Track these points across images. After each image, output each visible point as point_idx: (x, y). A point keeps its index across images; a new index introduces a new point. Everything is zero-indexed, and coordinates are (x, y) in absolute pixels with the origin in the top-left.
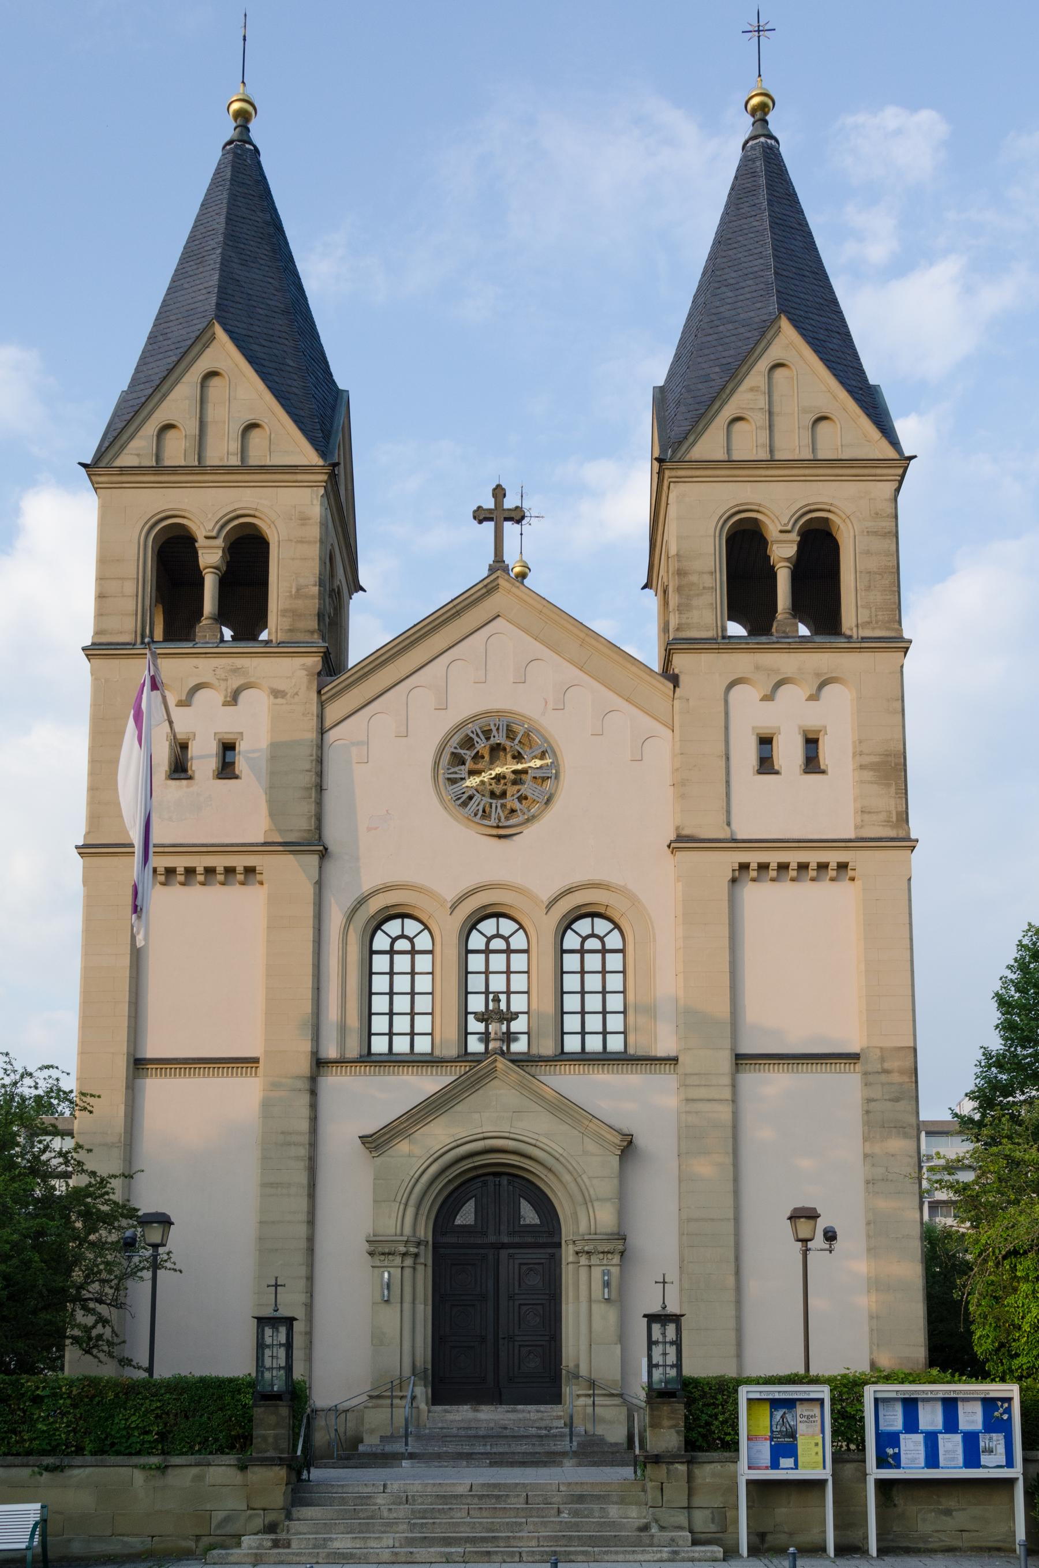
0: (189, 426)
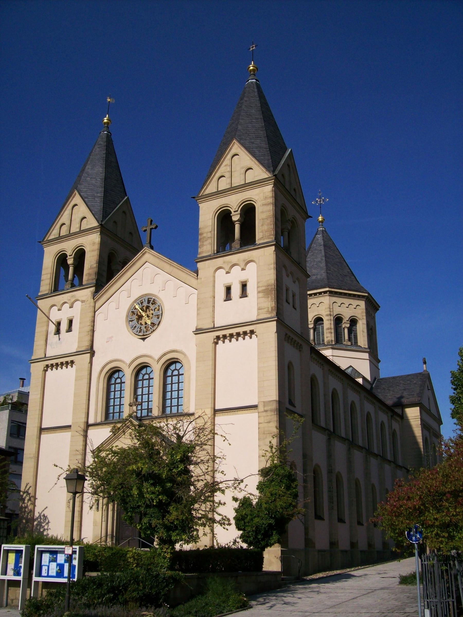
0: (68, 223)
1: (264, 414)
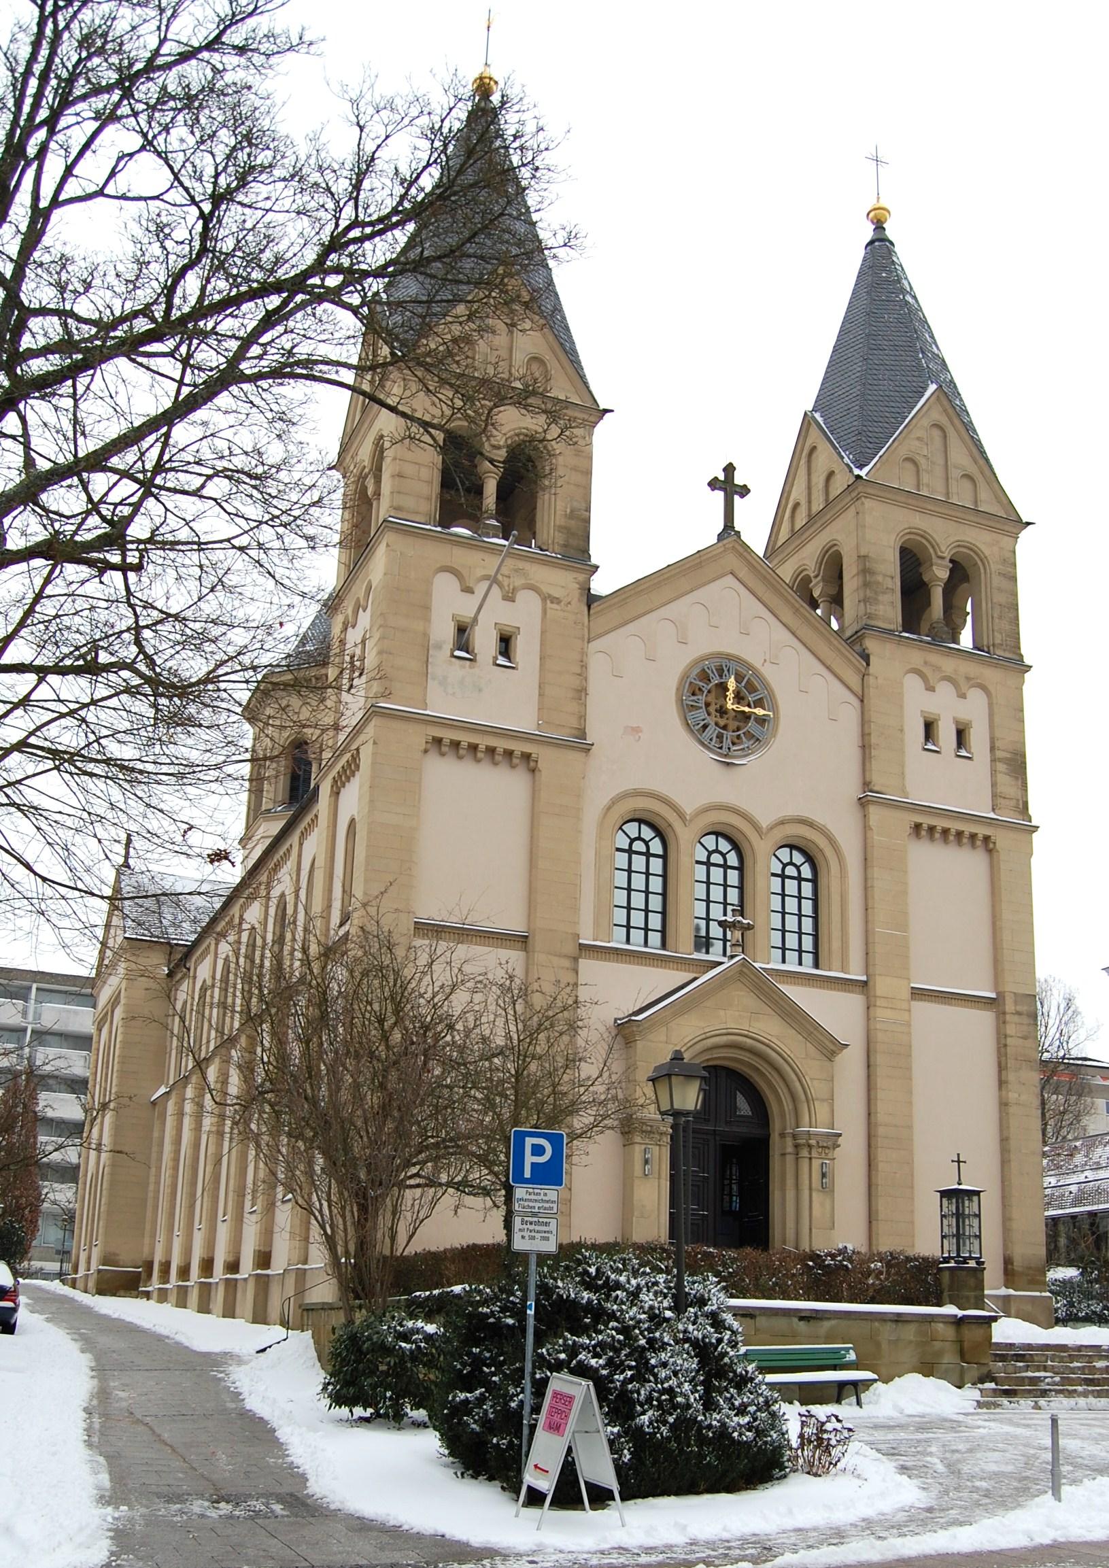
1: (1016, 1018)
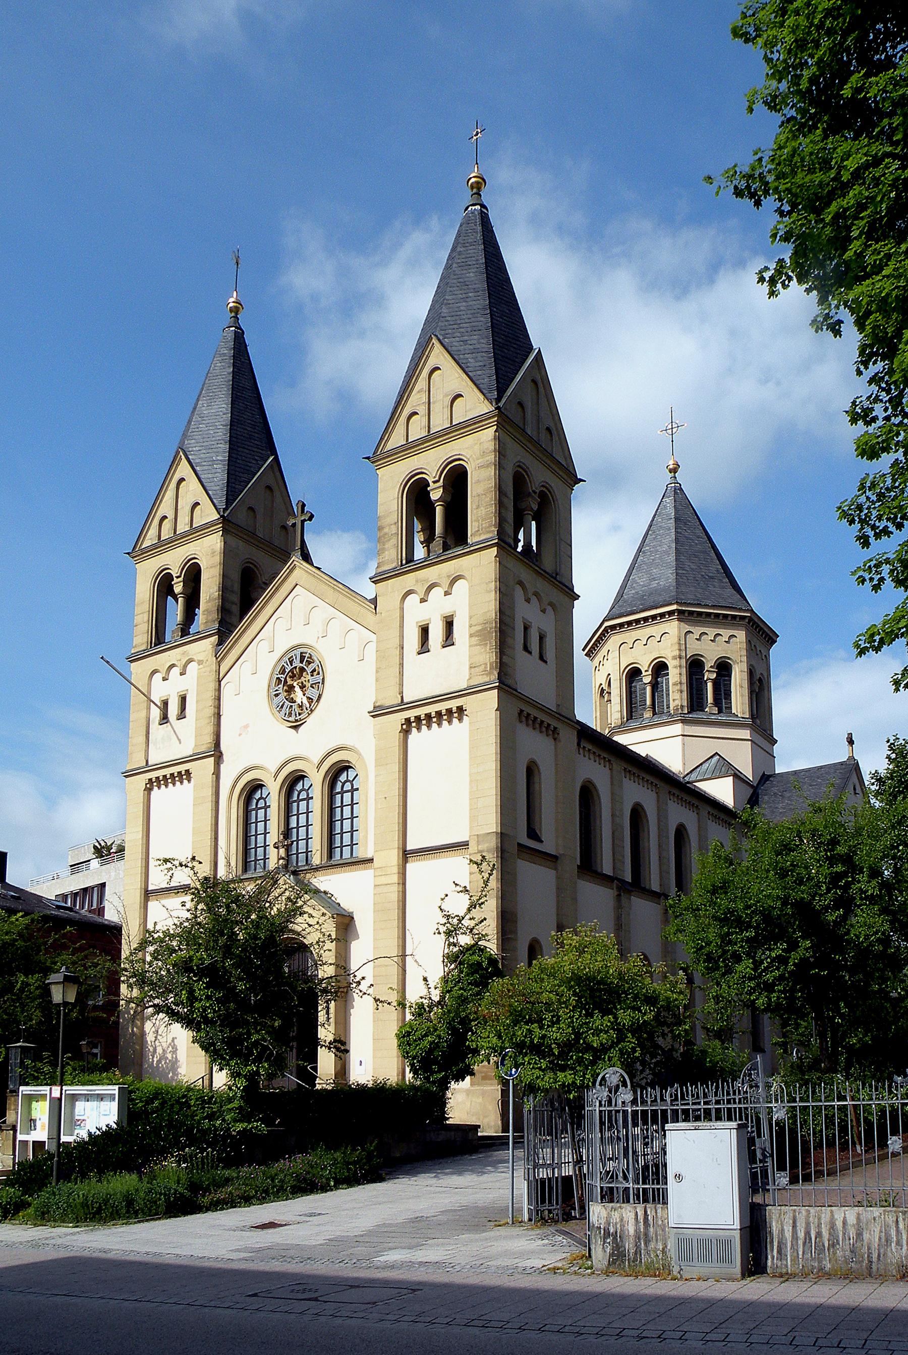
0: (171, 516)
